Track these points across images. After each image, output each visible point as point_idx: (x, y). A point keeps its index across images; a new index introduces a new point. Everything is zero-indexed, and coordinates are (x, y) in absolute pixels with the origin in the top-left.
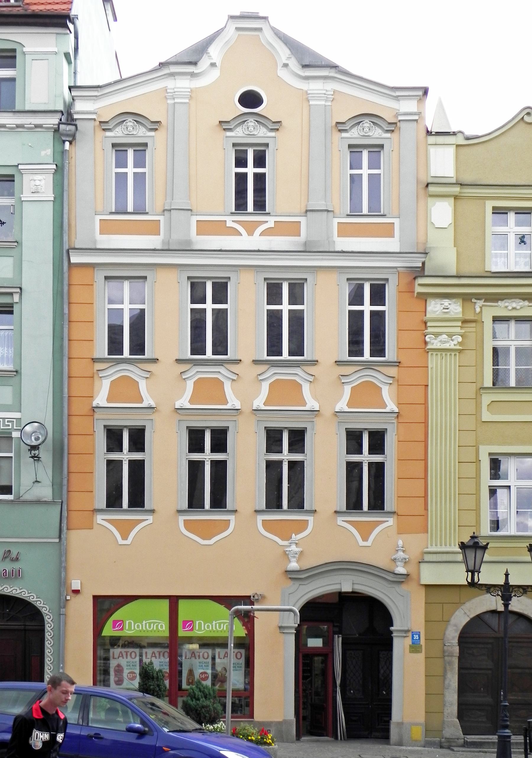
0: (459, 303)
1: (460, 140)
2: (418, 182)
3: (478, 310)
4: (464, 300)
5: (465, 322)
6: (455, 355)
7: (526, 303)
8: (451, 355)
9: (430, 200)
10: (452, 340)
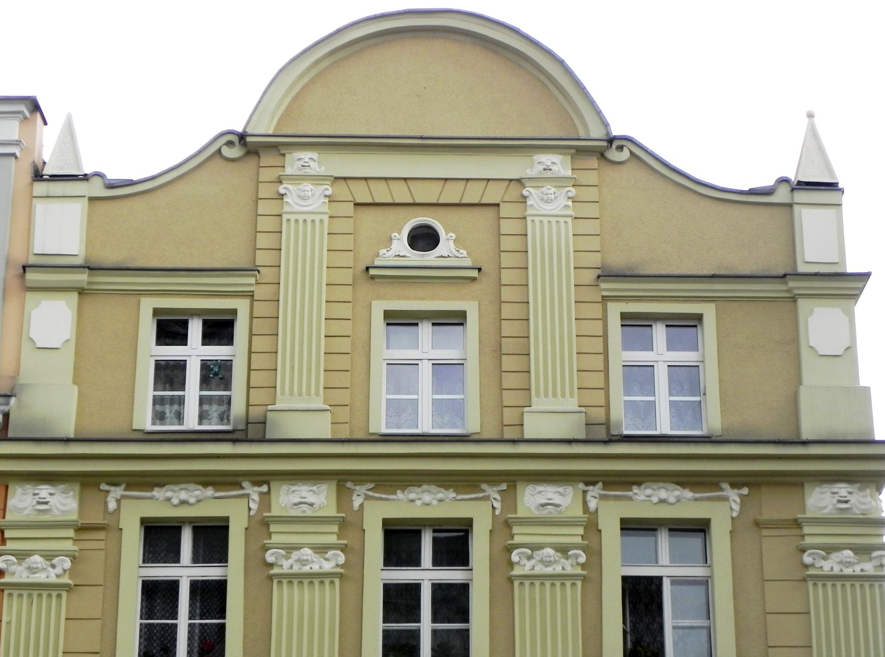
0: (72, 493)
1: (96, 189)
2: (8, 262)
3: (112, 505)
5: (82, 529)
6: (59, 596)
7: (210, 492)
8: (50, 596)
9: (30, 296)
10: (53, 566)
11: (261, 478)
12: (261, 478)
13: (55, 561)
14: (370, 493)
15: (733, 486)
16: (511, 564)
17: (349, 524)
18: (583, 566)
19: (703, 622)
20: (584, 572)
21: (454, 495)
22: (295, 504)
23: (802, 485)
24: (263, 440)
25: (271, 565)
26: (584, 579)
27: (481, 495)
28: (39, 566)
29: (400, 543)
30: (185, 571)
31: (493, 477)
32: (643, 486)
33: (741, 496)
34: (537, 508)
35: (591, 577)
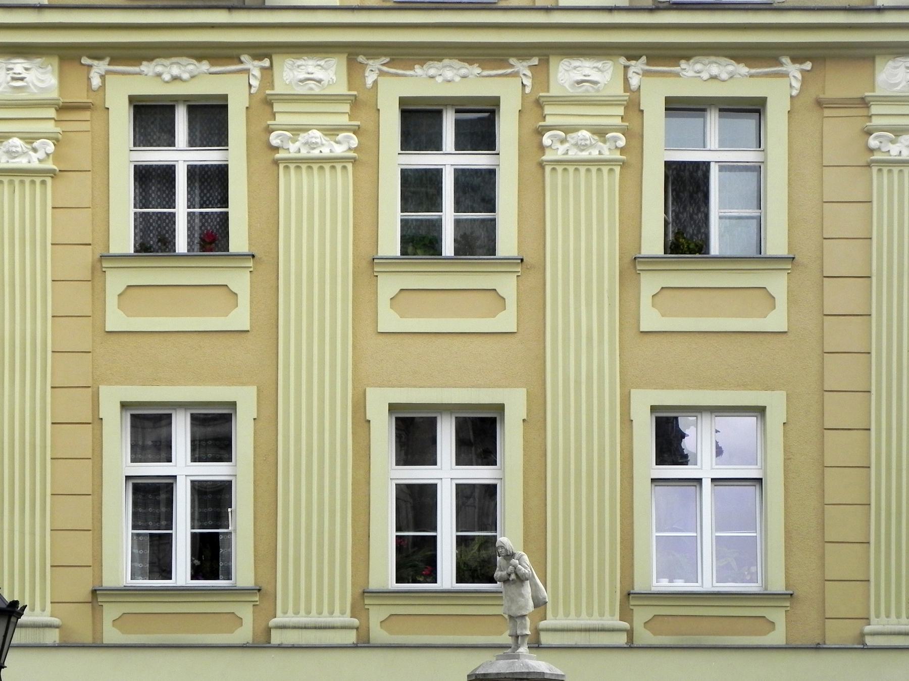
0: (50, 67)
3: (96, 82)
4: (63, 60)
5: (64, 108)
6: (43, 183)
7: (205, 66)
8: (33, 182)
10: (35, 150)
11: (261, 51)
12: (261, 51)
13: (36, 144)
14: (385, 69)
15: (795, 60)
16: (542, 148)
17: (361, 103)
18: (622, 150)
19: (754, 212)
20: (624, 157)
21: (479, 70)
22: (301, 81)
23: (872, 59)
25: (276, 149)
26: (624, 165)
27: (509, 71)
28: (19, 149)
29: (419, 123)
30: (182, 155)
31: (523, 51)
32: (692, 61)
33: (803, 72)
34: (572, 86)
35: (630, 164)
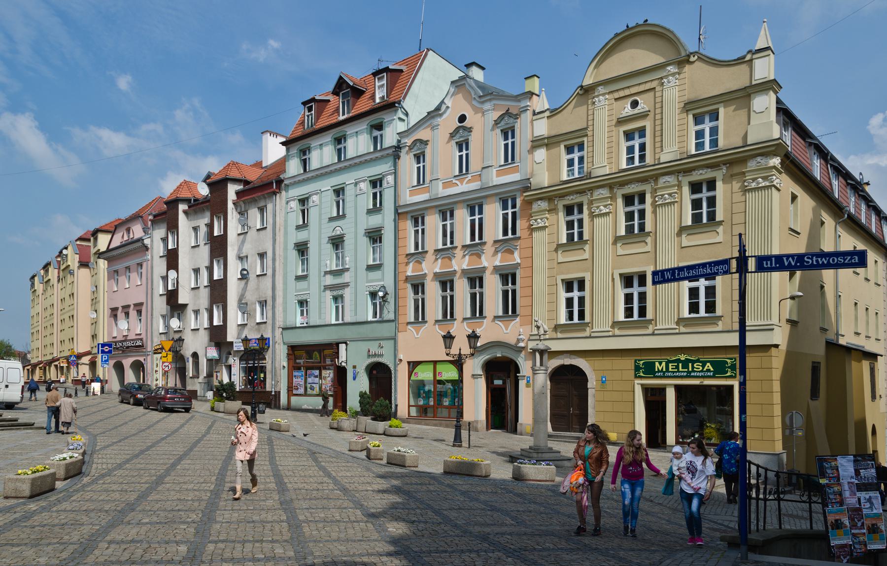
1: (547, 114)
24: (591, 178)
31: (651, 177)
